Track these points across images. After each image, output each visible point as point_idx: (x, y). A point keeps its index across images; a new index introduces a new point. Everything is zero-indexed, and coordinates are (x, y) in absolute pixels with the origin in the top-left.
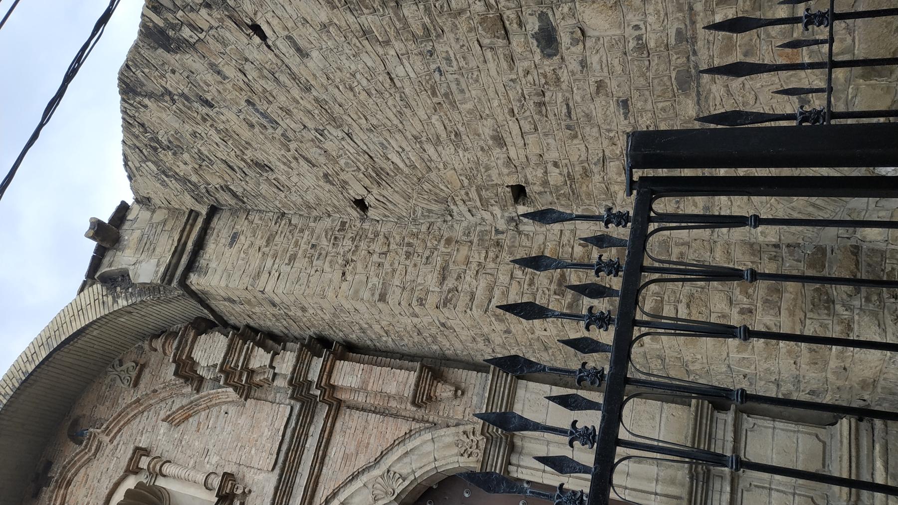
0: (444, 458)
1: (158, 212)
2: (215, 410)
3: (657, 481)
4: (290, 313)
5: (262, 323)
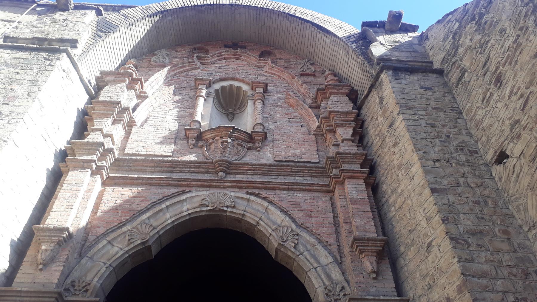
1: (420, 47)
2: (299, 120)
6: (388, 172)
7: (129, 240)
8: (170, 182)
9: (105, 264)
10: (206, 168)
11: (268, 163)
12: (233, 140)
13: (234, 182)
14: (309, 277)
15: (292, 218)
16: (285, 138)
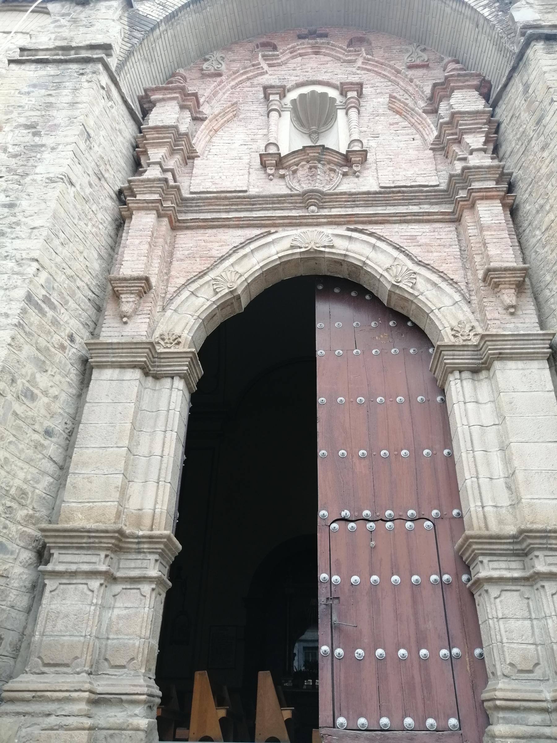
0: (444, 316)
2: (410, 131)
3: (496, 506)
4: (533, 142)
6: (533, 186)
8: (252, 222)
10: (292, 203)
11: (372, 190)
12: (324, 165)
14: (431, 319)
15: (407, 255)
16: (392, 157)
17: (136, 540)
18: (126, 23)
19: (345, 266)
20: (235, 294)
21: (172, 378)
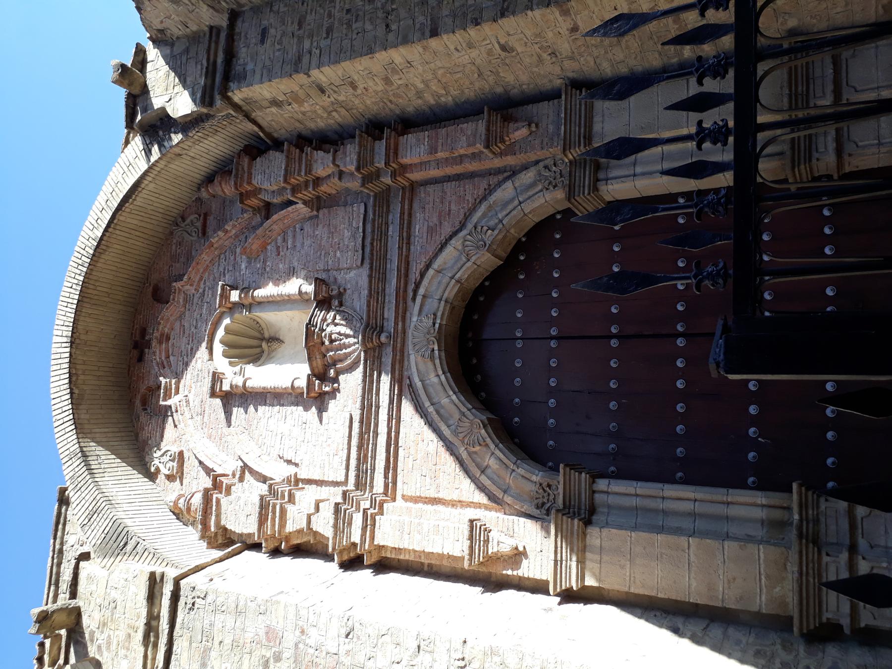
1: (177, 44)
2: (290, 234)
5: (312, 125)
7: (480, 445)
9: (513, 470)
13: (396, 318)
14: (530, 213)
17: (805, 523)
18: (112, 559)
19: (456, 303)
20: (486, 422)
21: (594, 492)
